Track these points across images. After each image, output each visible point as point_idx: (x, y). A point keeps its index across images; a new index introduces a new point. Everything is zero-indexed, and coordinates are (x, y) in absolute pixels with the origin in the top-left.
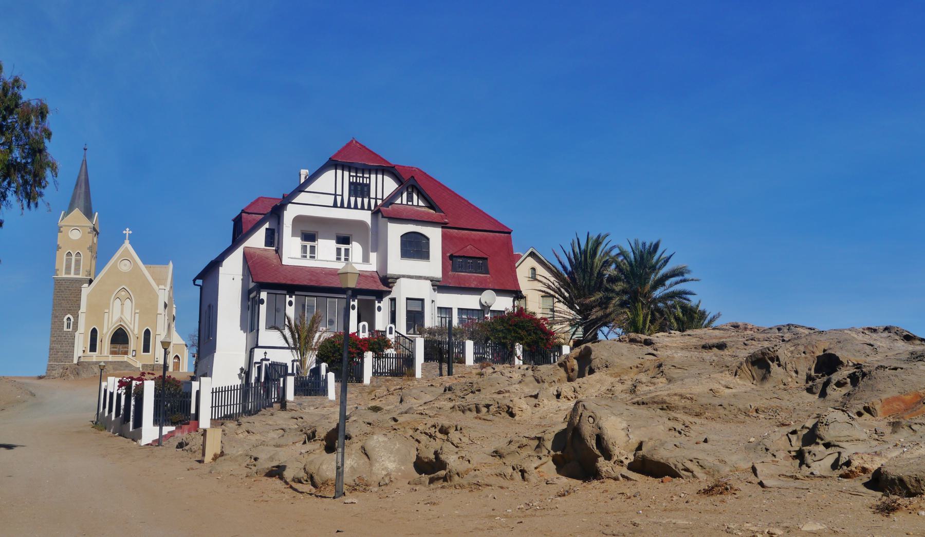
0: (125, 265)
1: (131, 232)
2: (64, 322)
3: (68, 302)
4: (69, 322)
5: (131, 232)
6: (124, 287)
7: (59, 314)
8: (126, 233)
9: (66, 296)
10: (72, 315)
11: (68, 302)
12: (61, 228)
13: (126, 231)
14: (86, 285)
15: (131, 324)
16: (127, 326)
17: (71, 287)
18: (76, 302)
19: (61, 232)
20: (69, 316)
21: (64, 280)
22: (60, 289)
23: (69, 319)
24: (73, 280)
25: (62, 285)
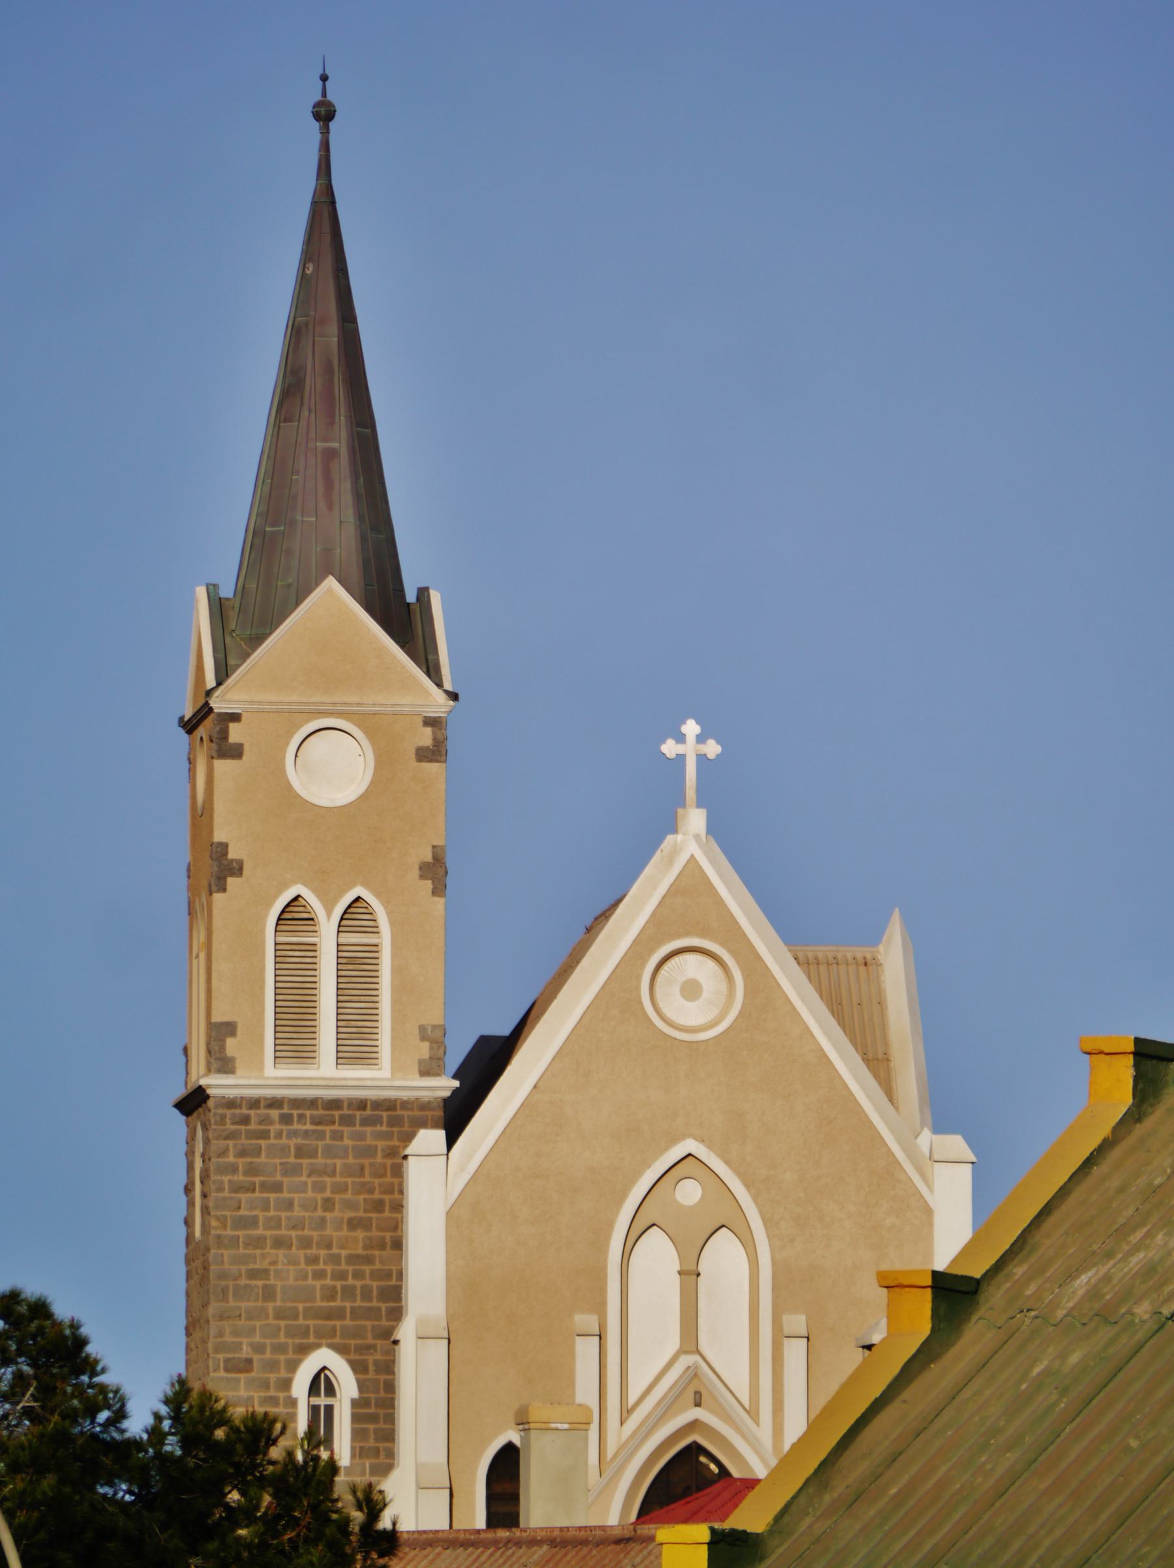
0: (691, 990)
1: (712, 749)
2: (293, 1403)
3: (314, 1260)
4: (322, 1401)
5: (712, 749)
6: (690, 1145)
7: (259, 1348)
8: (681, 758)
9: (297, 1212)
10: (341, 1350)
11: (314, 1260)
12: (232, 726)
13: (681, 738)
14: (431, 1138)
15: (753, 1412)
16: (744, 1437)
17: (329, 1152)
18: (369, 1260)
19: (236, 752)
20: (324, 1357)
21: (275, 1103)
22: (252, 1170)
23: (321, 1383)
24: (335, 1104)
25: (264, 1135)
